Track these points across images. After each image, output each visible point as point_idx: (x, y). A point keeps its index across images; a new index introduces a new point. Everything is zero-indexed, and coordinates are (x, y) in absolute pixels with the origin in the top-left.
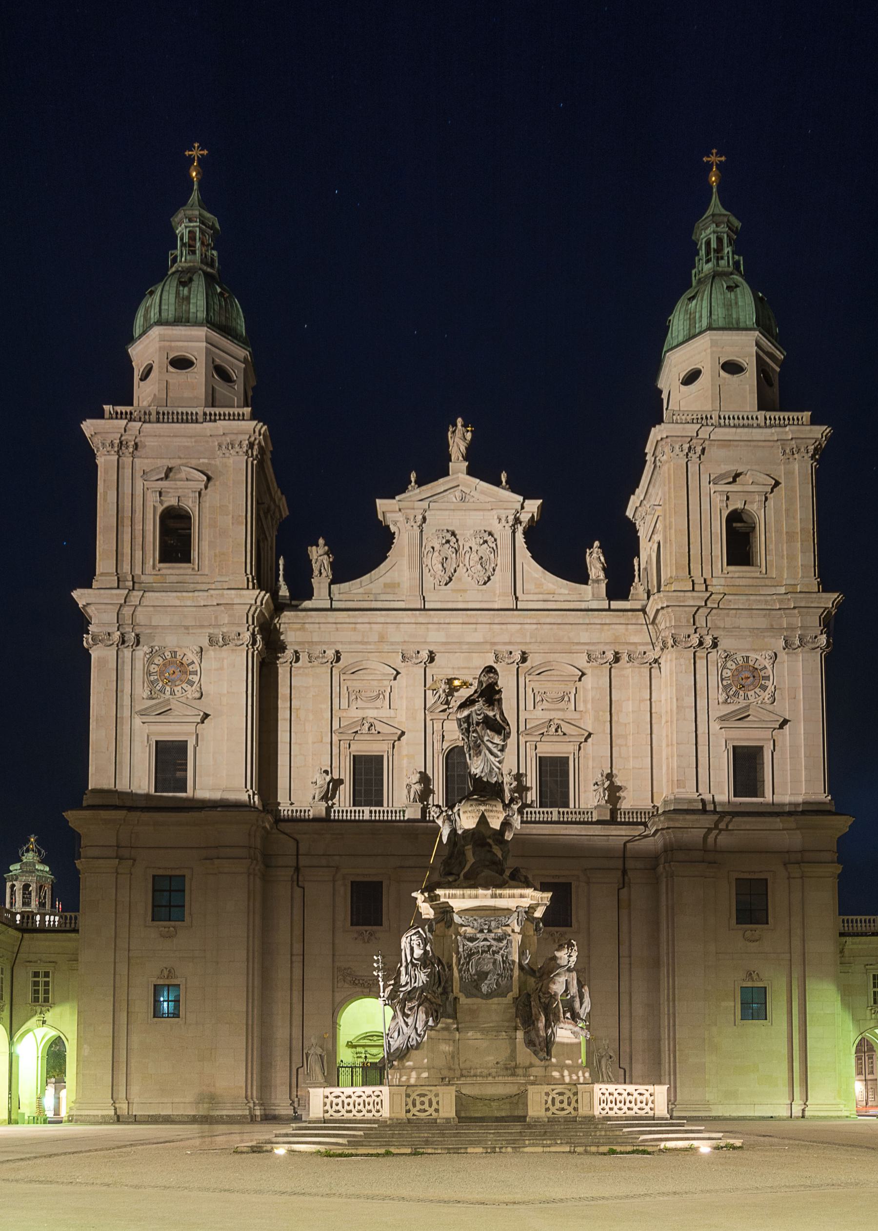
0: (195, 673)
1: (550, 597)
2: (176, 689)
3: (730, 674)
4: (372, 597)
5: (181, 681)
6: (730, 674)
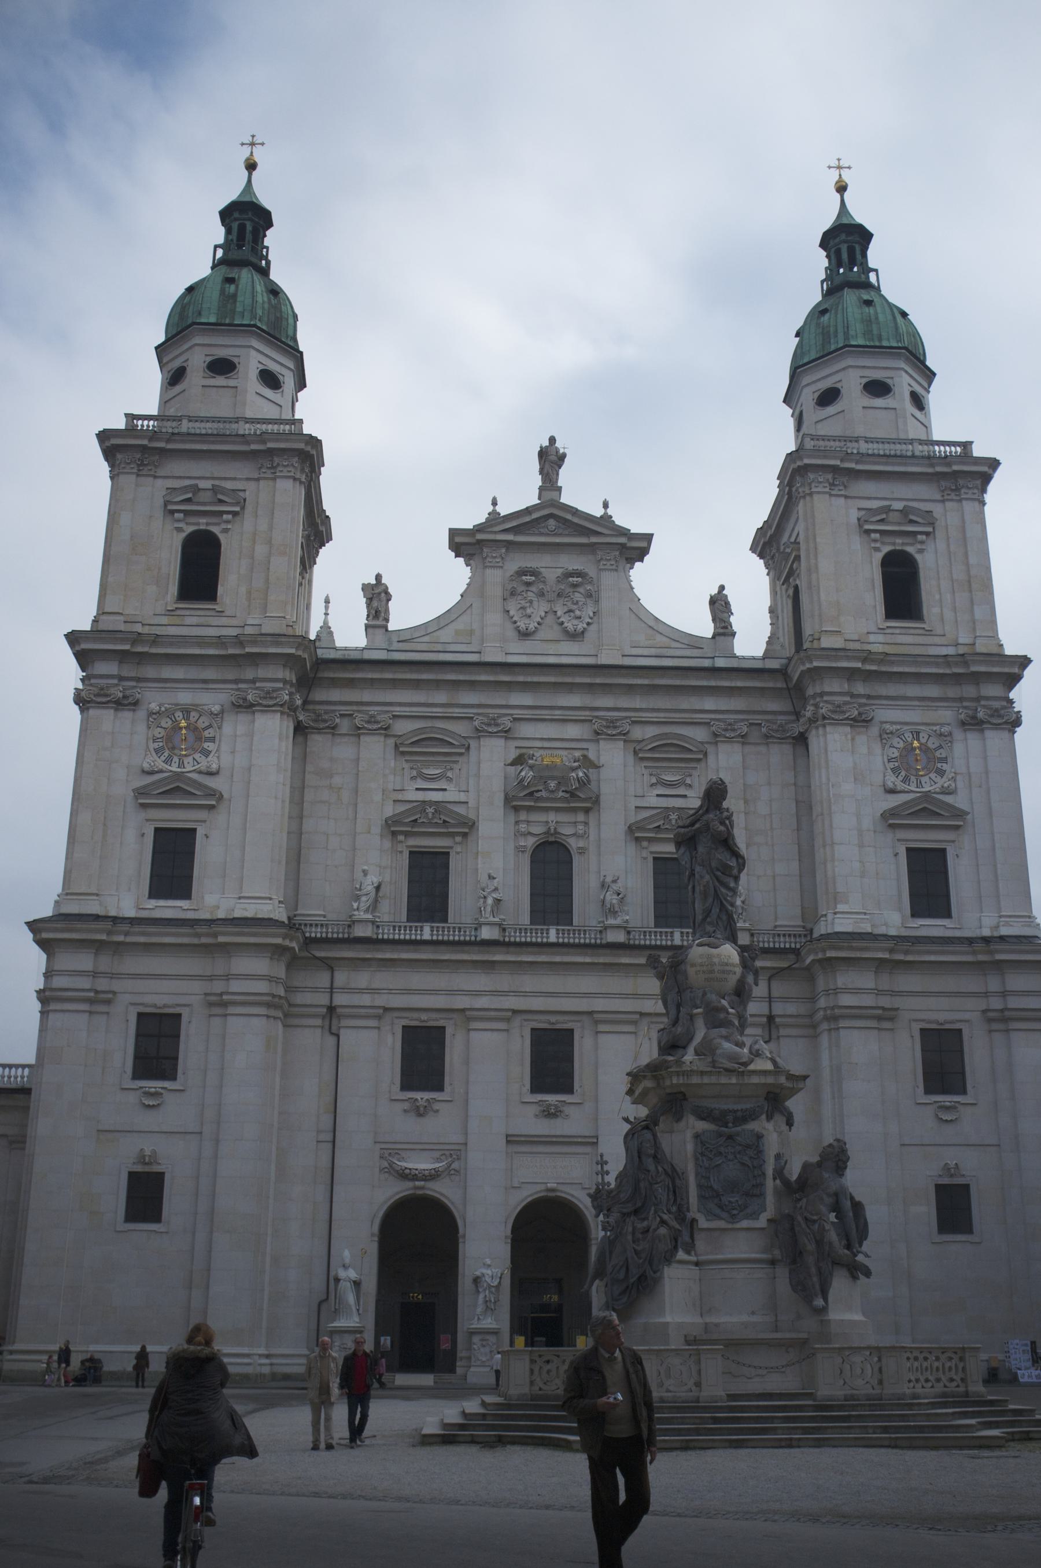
0: (212, 740)
1: (665, 652)
3: (896, 754)
4: (440, 647)
6: (896, 754)
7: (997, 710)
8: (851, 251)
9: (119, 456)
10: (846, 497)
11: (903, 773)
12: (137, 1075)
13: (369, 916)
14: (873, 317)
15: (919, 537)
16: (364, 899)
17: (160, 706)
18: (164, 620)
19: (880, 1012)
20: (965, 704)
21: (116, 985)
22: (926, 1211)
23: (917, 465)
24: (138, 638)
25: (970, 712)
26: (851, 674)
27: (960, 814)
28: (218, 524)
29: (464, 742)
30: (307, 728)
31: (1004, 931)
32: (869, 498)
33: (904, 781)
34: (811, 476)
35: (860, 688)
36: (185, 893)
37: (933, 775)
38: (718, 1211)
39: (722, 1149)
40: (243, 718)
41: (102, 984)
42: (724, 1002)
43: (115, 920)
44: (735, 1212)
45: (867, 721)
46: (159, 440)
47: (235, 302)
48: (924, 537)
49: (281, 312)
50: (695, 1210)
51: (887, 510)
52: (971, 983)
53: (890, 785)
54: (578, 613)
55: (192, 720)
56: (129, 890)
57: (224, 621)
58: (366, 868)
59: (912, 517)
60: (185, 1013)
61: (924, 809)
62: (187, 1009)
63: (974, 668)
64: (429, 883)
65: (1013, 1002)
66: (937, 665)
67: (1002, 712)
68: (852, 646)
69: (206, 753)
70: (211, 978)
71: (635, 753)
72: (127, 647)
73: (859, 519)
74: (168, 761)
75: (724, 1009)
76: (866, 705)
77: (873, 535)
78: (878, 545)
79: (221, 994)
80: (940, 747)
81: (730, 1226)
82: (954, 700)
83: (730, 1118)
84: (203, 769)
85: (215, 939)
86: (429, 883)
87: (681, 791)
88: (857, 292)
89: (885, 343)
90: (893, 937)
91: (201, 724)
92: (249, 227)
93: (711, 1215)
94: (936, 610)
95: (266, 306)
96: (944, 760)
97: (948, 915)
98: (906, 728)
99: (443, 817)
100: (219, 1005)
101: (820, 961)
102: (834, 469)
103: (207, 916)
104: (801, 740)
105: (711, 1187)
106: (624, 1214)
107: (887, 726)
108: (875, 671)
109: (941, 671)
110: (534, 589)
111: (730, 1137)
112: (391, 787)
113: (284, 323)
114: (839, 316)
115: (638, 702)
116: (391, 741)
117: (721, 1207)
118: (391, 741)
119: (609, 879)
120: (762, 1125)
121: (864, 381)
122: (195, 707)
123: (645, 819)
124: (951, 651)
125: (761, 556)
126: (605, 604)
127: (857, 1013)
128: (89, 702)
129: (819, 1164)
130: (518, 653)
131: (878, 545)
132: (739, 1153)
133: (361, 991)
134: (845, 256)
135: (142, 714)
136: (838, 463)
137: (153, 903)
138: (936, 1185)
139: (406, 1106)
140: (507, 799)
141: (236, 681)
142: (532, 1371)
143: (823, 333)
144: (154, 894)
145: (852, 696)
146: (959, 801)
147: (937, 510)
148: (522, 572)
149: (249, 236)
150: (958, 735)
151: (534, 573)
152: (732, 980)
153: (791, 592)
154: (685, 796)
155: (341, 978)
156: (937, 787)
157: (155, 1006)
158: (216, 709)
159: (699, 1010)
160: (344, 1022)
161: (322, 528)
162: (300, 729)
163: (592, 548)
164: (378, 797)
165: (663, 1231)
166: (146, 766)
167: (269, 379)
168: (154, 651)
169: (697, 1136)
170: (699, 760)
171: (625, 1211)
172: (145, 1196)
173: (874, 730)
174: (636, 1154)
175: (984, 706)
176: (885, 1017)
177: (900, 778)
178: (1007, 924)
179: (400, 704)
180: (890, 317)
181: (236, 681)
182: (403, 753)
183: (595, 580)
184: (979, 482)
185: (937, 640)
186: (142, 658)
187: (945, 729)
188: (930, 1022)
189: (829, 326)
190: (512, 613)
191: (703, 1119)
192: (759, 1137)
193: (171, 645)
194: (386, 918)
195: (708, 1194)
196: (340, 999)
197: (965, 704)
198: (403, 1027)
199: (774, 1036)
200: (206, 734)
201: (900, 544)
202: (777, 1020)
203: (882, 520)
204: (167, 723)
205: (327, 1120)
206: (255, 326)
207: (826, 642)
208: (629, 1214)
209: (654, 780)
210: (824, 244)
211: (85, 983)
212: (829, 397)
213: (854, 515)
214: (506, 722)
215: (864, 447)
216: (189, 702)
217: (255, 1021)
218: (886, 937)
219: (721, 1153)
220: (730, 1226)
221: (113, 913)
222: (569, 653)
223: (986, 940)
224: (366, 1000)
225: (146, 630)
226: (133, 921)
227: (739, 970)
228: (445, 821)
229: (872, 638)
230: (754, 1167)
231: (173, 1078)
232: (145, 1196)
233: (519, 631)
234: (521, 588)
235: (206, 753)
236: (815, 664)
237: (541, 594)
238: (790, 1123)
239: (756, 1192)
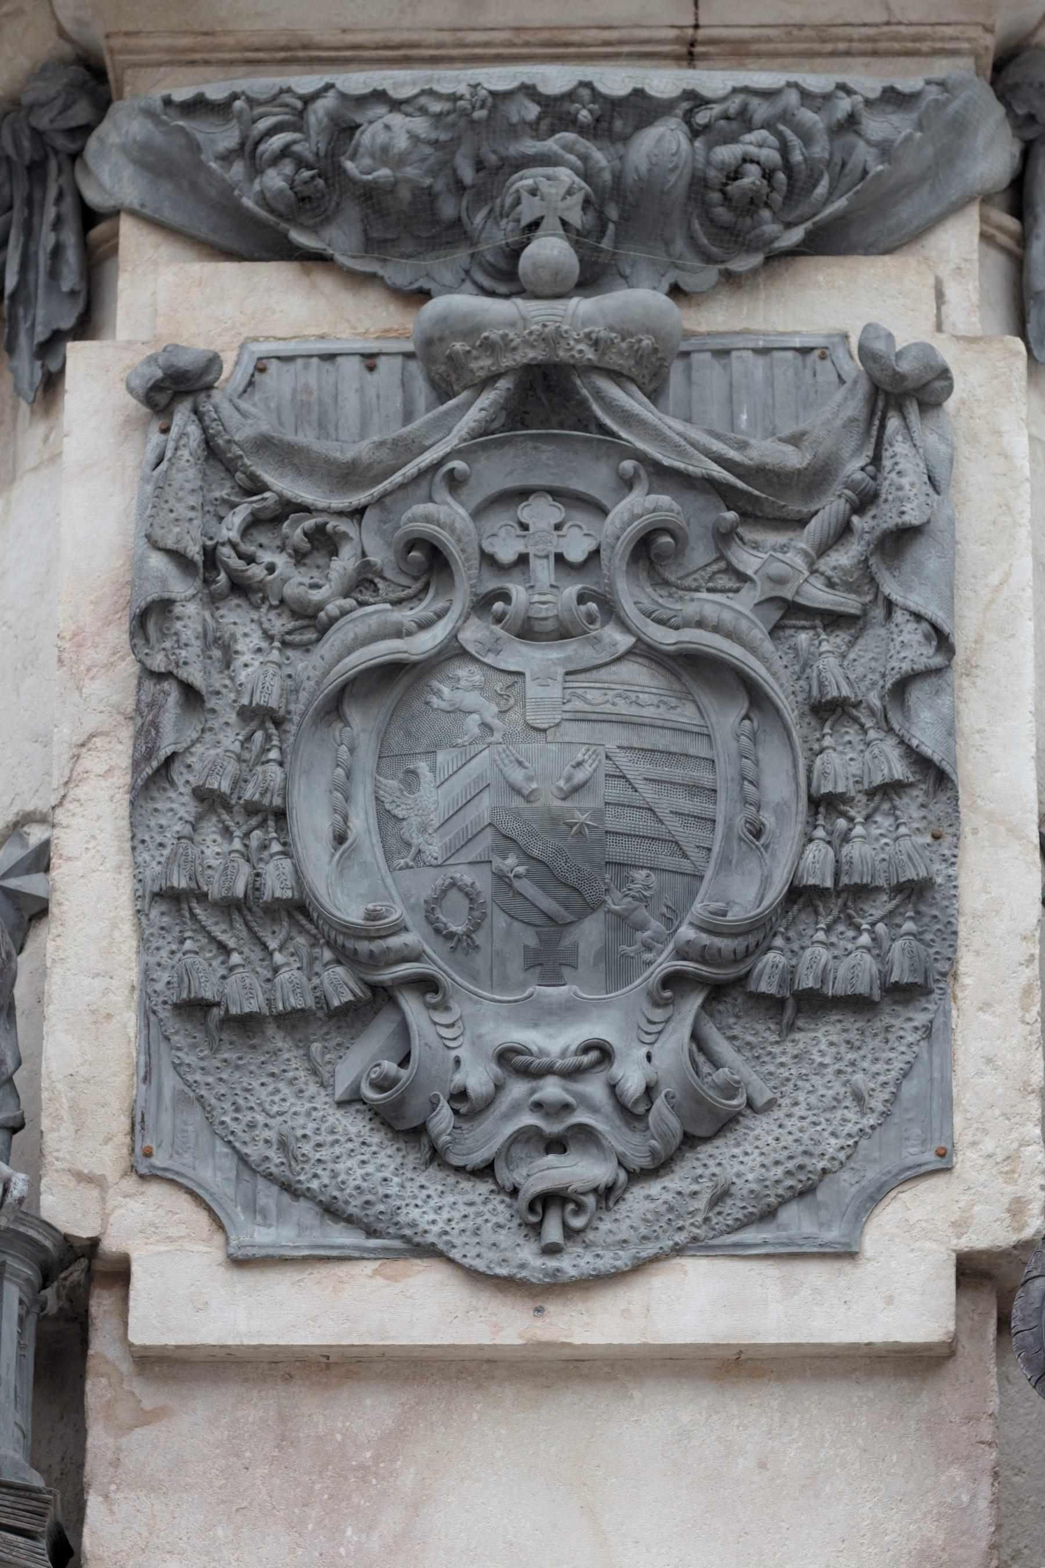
38: (364, 1163)
39: (446, 515)
50: (107, 1156)
81: (503, 1325)
105: (299, 910)
111: (546, 396)
117: (399, 1120)
132: (648, 551)
169: (174, 388)
192: (901, 392)
219: (430, 562)
220: (503, 1325)
230: (829, 710)
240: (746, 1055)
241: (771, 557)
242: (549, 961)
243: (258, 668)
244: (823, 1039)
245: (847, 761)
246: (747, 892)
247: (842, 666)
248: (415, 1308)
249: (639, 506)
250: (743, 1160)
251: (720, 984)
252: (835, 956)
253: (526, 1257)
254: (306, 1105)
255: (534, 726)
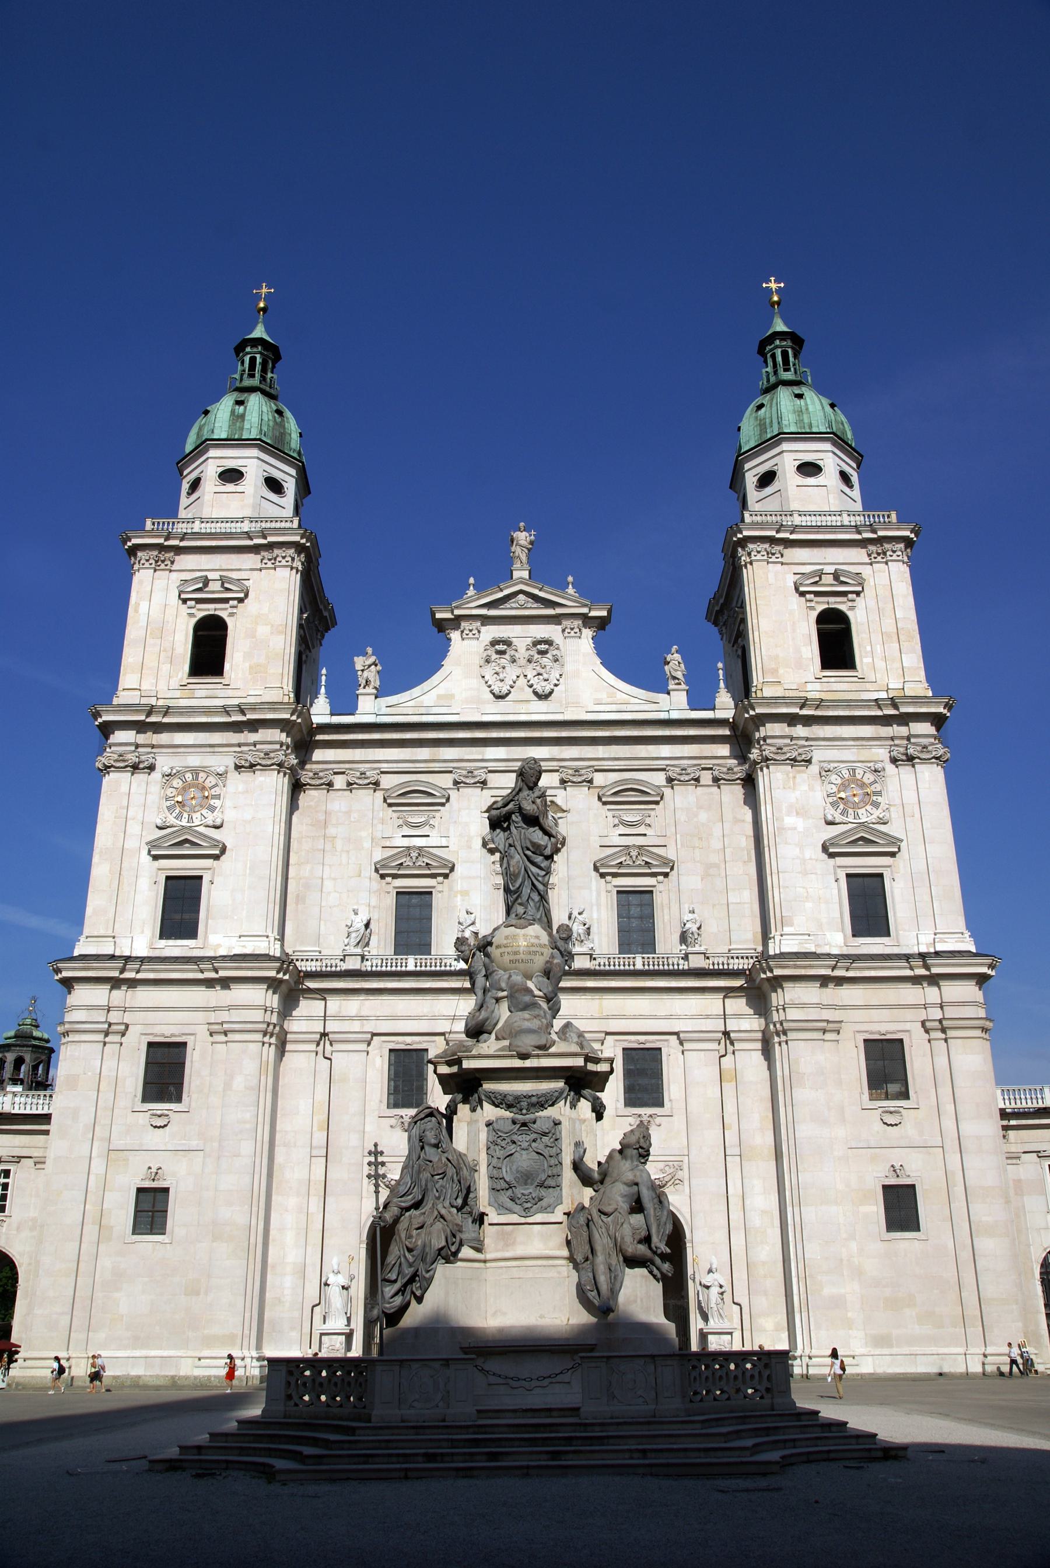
1: (623, 707)
2: (195, 816)
5: (201, 806)
7: (925, 747)
8: (785, 354)
9: (139, 554)
10: (782, 564)
11: (842, 806)
12: (145, 1099)
13: (358, 950)
14: (804, 408)
15: (850, 596)
16: (353, 935)
17: (172, 769)
18: (178, 694)
19: (825, 1024)
20: (897, 742)
21: (128, 1018)
22: (877, 1210)
23: (846, 532)
24: (151, 711)
25: (902, 750)
26: (792, 720)
27: (895, 841)
28: (226, 609)
29: (444, 793)
30: (305, 785)
31: (940, 947)
32: (804, 564)
33: (842, 814)
34: (751, 546)
35: (800, 731)
36: (191, 932)
37: (869, 807)
38: (510, 1204)
39: (515, 1137)
40: (247, 776)
41: (114, 1017)
42: (530, 985)
43: (128, 959)
44: (529, 1205)
45: (806, 761)
46: (175, 538)
47: (243, 421)
48: (854, 595)
49: (284, 428)
50: (486, 1203)
51: (820, 574)
52: (910, 994)
53: (830, 818)
54: (546, 676)
55: (201, 780)
56: (142, 932)
57: (230, 693)
58: (355, 907)
59: (842, 579)
60: (190, 1040)
61: (862, 838)
62: (192, 1037)
63: (904, 709)
64: (413, 919)
65: (950, 1012)
66: (869, 707)
67: (930, 748)
68: (788, 694)
69: (212, 809)
70: (215, 1009)
71: (600, 799)
72: (142, 718)
73: (795, 584)
74: (179, 817)
75: (529, 991)
76: (805, 746)
77: (808, 596)
78: (812, 604)
79: (222, 1024)
80: (875, 782)
81: (523, 1220)
82: (886, 739)
83: (524, 1104)
84: (211, 823)
85: (217, 975)
86: (413, 919)
87: (642, 830)
88: (790, 388)
89: (814, 430)
90: (835, 956)
91: (208, 784)
92: (259, 360)
93: (502, 1209)
94: (867, 660)
95: (271, 423)
96: (879, 793)
97: (889, 935)
98: (842, 765)
99: (426, 860)
100: (221, 1032)
101: (768, 979)
102: (771, 540)
103: (211, 954)
104: (749, 782)
106: (402, 1209)
107: (825, 765)
108: (813, 716)
109: (873, 713)
110: (507, 656)
111: (524, 1124)
112: (379, 835)
113: (287, 437)
114: (774, 409)
115: (601, 751)
116: (379, 795)
118: (379, 795)
119: (575, 913)
120: (561, 1111)
121: (798, 463)
122: (203, 769)
123: (608, 856)
124: (883, 695)
125: (715, 623)
126: (569, 667)
127: (805, 1026)
128: (109, 767)
129: (621, 1152)
130: (494, 712)
131: (812, 604)
132: (534, 1141)
133: (351, 1018)
134: (779, 359)
135: (156, 775)
136: (772, 533)
137: (164, 943)
138: (884, 1187)
139: (393, 1121)
140: (484, 844)
141: (239, 745)
142: (289, 1383)
143: (760, 425)
144: (163, 935)
145: (792, 738)
146: (893, 829)
147: (866, 571)
148: (494, 643)
149: (258, 367)
150: (890, 768)
151: (508, 643)
152: (539, 962)
153: (740, 652)
154: (645, 835)
155: (334, 1004)
156: (873, 818)
157: (163, 1035)
158: (221, 770)
159: (505, 993)
160: (337, 1047)
161: (326, 614)
162: (297, 787)
163: (556, 619)
164: (367, 844)
165: (439, 1225)
166: (159, 823)
167: (274, 485)
168: (166, 720)
170: (657, 803)
171: (403, 1205)
172: (151, 1209)
173: (814, 768)
174: (418, 1145)
175: (914, 744)
176: (829, 1029)
177: (839, 811)
178: (942, 941)
179: (387, 762)
180: (819, 407)
181: (239, 745)
182: (390, 805)
183: (561, 647)
184: (902, 546)
185: (869, 686)
186: (158, 728)
187: (879, 766)
188: (872, 1033)
189: (765, 419)
190: (486, 678)
191: (497, 1106)
192: (557, 1124)
193: (181, 714)
194: (374, 952)
195: (500, 1186)
196: (331, 1027)
197: (897, 742)
198: (391, 1050)
199: (730, 1048)
200: (213, 792)
201: (834, 603)
202: (732, 1035)
203: (816, 583)
204: (177, 783)
205: (320, 1137)
206: (259, 440)
207: (768, 692)
208: (408, 1209)
209: (616, 821)
210: (761, 351)
211: (101, 1016)
212: (767, 479)
213: (790, 580)
214: (481, 775)
215: (797, 520)
216: (197, 764)
217: (252, 1045)
218: (829, 956)
219: (514, 1142)
221: (127, 954)
222: (539, 711)
223: (923, 956)
224: (356, 1026)
225: (161, 703)
226: (143, 960)
227: (548, 952)
228: (427, 864)
229: (809, 687)
231: (179, 1099)
232: (151, 1209)
233: (494, 694)
234: (494, 656)
235: (212, 809)
236: (759, 710)
237: (514, 661)
238: (599, 1112)
239: (549, 1183)
240: (543, 1192)
241: (545, 1139)
242: (526, 1184)
243: (500, 1153)
244: (551, 1190)
245: (553, 1161)
246: (543, 1177)
247: (553, 1151)
248: (514, 1218)
249: (534, 1136)
250: (543, 1203)
251: (541, 1185)
252: (550, 1182)
253: (524, 1214)
254: (504, 1197)
255: (524, 1160)
